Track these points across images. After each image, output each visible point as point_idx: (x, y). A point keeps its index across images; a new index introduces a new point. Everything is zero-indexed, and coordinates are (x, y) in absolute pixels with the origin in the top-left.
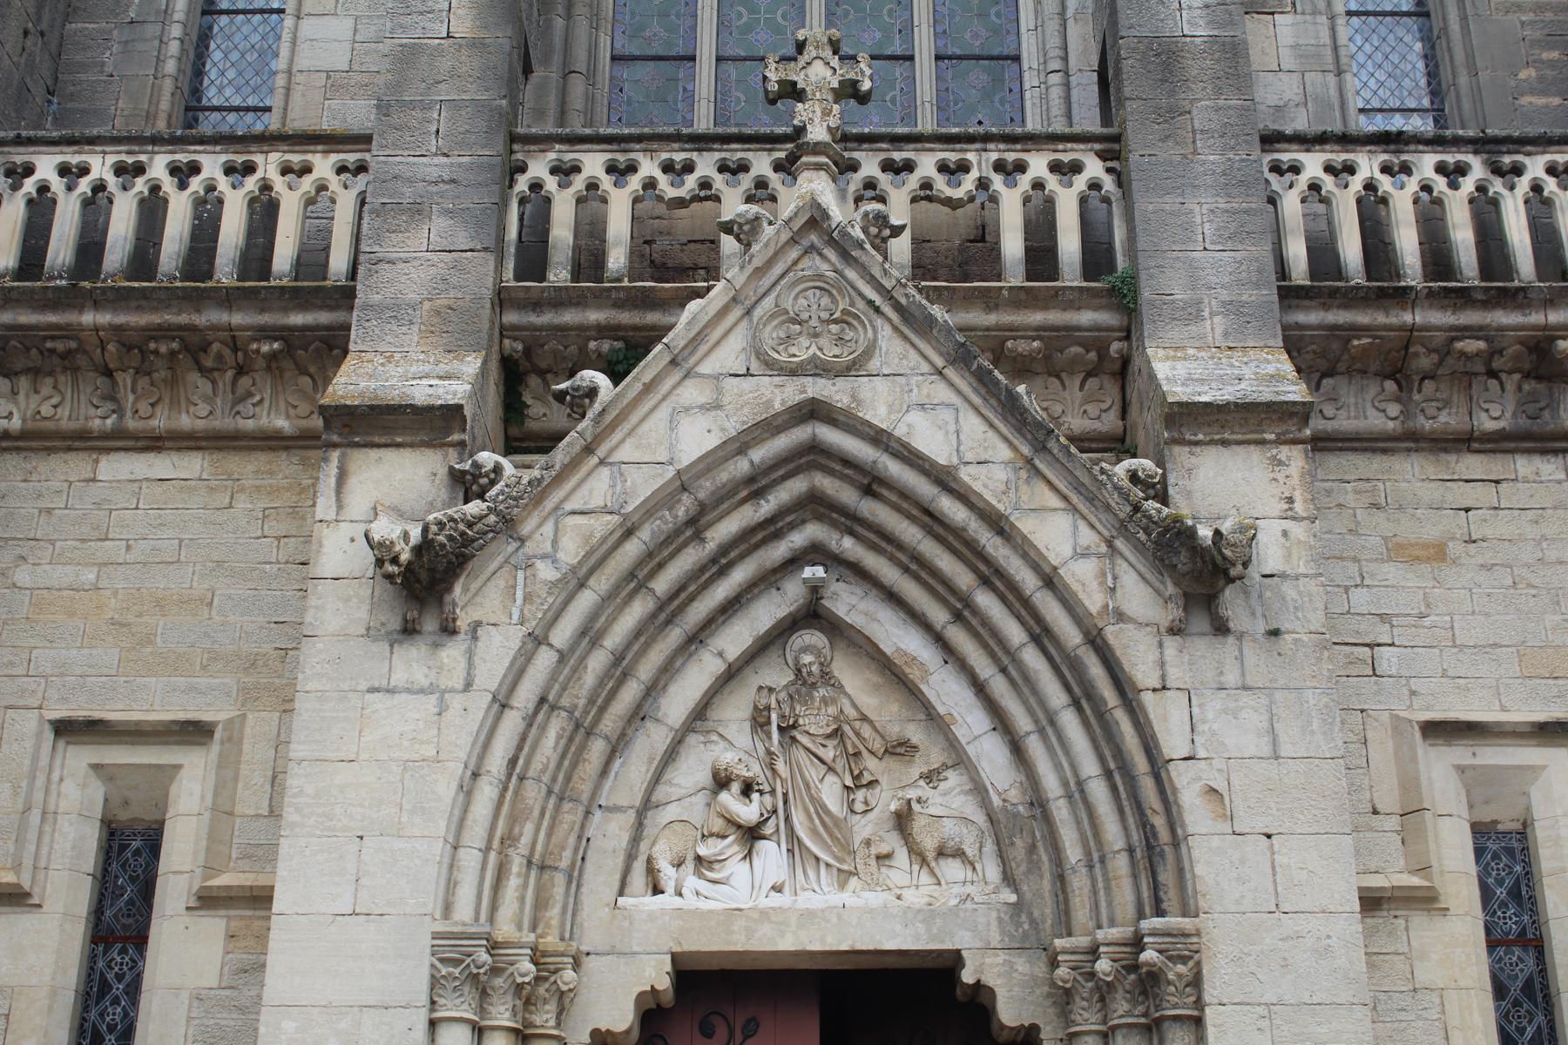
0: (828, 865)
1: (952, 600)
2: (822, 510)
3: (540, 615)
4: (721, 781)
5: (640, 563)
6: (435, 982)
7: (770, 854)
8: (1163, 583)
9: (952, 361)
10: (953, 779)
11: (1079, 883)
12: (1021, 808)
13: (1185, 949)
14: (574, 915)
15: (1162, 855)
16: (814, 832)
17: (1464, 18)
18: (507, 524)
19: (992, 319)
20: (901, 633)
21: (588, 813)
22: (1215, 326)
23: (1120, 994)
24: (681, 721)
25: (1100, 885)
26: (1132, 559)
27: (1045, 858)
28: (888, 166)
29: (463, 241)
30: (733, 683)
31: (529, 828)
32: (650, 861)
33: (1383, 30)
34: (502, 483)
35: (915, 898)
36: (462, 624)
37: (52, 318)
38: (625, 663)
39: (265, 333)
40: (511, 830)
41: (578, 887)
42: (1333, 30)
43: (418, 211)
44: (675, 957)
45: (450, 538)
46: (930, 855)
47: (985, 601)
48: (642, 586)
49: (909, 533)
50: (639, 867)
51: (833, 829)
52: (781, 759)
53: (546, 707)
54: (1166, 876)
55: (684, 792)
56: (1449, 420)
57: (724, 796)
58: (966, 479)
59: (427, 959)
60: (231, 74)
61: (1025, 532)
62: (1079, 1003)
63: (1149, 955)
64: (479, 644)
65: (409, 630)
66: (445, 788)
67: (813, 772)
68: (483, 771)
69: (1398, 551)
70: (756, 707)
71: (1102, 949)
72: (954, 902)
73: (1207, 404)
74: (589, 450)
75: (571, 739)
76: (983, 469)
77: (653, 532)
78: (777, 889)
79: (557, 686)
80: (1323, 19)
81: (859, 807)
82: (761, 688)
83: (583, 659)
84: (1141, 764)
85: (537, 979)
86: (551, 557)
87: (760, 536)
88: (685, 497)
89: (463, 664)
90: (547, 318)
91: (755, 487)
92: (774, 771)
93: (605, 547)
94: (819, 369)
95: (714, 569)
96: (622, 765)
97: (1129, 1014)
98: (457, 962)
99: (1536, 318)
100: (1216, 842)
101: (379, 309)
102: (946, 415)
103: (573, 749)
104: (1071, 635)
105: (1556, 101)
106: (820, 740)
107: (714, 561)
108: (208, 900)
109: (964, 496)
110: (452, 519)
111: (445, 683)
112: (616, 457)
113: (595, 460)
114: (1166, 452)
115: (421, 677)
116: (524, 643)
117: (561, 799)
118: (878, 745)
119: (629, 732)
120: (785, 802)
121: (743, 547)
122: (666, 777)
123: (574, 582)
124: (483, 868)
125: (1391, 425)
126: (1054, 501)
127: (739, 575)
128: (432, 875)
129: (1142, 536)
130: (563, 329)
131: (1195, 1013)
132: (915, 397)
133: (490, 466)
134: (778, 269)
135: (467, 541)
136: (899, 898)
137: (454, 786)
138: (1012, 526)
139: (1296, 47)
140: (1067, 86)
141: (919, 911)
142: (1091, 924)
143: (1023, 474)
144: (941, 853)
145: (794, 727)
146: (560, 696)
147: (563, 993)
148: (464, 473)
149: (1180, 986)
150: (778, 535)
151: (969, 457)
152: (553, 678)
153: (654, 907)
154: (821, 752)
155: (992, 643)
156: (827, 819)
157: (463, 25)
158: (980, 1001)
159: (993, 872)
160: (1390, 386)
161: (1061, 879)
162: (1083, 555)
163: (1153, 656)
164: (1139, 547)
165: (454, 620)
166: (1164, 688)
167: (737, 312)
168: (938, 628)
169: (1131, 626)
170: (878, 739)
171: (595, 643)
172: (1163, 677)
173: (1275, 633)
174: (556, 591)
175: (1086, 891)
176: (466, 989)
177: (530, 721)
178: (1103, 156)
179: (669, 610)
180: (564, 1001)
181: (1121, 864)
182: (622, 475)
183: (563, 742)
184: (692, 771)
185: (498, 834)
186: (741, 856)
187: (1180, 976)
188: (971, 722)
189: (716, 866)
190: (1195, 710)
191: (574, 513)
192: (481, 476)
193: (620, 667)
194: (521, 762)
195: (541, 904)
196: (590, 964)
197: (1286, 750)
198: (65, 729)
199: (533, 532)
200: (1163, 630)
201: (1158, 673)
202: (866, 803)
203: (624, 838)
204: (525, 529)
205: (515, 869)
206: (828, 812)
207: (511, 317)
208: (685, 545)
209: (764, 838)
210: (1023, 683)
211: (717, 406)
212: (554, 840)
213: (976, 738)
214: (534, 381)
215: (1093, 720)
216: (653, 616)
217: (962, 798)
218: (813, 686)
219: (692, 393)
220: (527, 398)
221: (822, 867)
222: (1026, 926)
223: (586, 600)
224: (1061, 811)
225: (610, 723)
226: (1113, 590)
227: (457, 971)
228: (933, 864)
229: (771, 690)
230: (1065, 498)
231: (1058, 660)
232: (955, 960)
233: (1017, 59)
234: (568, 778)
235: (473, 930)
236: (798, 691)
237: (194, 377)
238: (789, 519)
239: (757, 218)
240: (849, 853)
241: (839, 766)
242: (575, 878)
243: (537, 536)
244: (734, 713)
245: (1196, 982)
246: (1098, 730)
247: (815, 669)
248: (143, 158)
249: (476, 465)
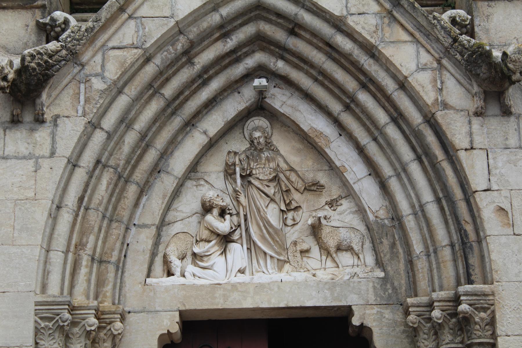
0: (271, 257)
1: (344, 97)
2: (265, 44)
3: (95, 111)
5: (155, 78)
6: (37, 331)
8: (472, 85)
10: (346, 205)
11: (421, 265)
12: (386, 222)
14: (120, 289)
15: (471, 248)
16: (263, 238)
20: (313, 118)
21: (127, 229)
23: (446, 331)
24: (182, 173)
25: (434, 266)
26: (452, 71)
27: (401, 251)
30: (213, 149)
31: (92, 239)
32: (165, 256)
34: (69, 31)
36: (48, 116)
38: (147, 139)
40: (81, 239)
41: (123, 273)
44: (181, 313)
45: (39, 64)
46: (332, 250)
47: (364, 97)
48: (157, 92)
50: (159, 260)
52: (243, 194)
53: (100, 166)
54: (474, 260)
55: (185, 215)
57: (209, 218)
58: (352, 24)
59: (32, 318)
61: (388, 56)
63: (464, 307)
64: (59, 129)
67: (262, 202)
68: (63, 205)
70: (227, 164)
71: (436, 304)
72: (347, 277)
75: (116, 185)
76: (361, 18)
77: (162, 59)
78: (242, 271)
79: (106, 154)
81: (290, 222)
82: (229, 152)
83: (122, 136)
84: (458, 194)
85: (99, 328)
86: (101, 76)
87: (227, 61)
88: (181, 37)
89: (49, 141)
91: (224, 31)
92: (238, 202)
93: (133, 69)
95: (200, 81)
96: (147, 200)
97: (452, 342)
98: (50, 319)
100: (503, 239)
103: (117, 191)
106: (265, 183)
107: (199, 76)
109: (351, 35)
110: (39, 53)
111: (38, 153)
112: (139, 14)
113: (125, 16)
114: (474, 5)
115: (23, 149)
116: (86, 128)
117: (111, 221)
118: (300, 185)
119: (151, 180)
120: (246, 220)
121: (217, 68)
122: (174, 206)
123: (115, 90)
124: (65, 263)
126: (404, 36)
127: (215, 85)
129: (458, 57)
131: (492, 341)
133: (61, 20)
135: (49, 66)
136: (314, 275)
137: (46, 214)
138: (380, 52)
141: (326, 283)
142: (429, 289)
143: (386, 20)
144: (339, 249)
145: (250, 175)
146: (108, 159)
147: (114, 336)
148: (45, 24)
149: (483, 325)
150: (238, 60)
151: (353, 10)
152: (104, 148)
153: (168, 284)
154: (266, 190)
155: (368, 123)
156: (270, 230)
159: (369, 259)
161: (410, 263)
162: (423, 69)
163: (465, 129)
164: (456, 63)
165: (43, 115)
166: (472, 148)
168: (336, 114)
169: (452, 112)
170: (300, 181)
171: (129, 127)
172: (471, 142)
174: (104, 96)
175: (426, 270)
176: (57, 335)
181: (446, 253)
182: (142, 24)
183: (111, 187)
185: (73, 242)
186: (219, 252)
187: (482, 319)
189: (205, 259)
190: (491, 161)
191: (114, 48)
192: (56, 26)
194: (86, 199)
195: (100, 283)
196: (131, 318)
199: (89, 60)
200: (471, 113)
201: (468, 139)
202: (294, 220)
203: (150, 243)
204: (85, 58)
205: (84, 263)
206: (271, 226)
208: (182, 67)
209: (233, 241)
212: (107, 245)
213: (359, 180)
215: (429, 168)
216: (164, 110)
217: (351, 216)
218: (261, 150)
221: (268, 258)
222: (390, 291)
223: (123, 101)
224: (410, 223)
225: (139, 175)
226: (441, 90)
227: (50, 325)
228: (334, 255)
229: (236, 153)
230: (412, 35)
231: (408, 132)
232: (348, 311)
234: (115, 208)
235: (60, 299)
236: (252, 154)
238: (244, 50)
240: (284, 250)
241: (277, 198)
243: (92, 63)
245: (492, 322)
246: (432, 174)
247: (262, 140)
249: (53, 20)
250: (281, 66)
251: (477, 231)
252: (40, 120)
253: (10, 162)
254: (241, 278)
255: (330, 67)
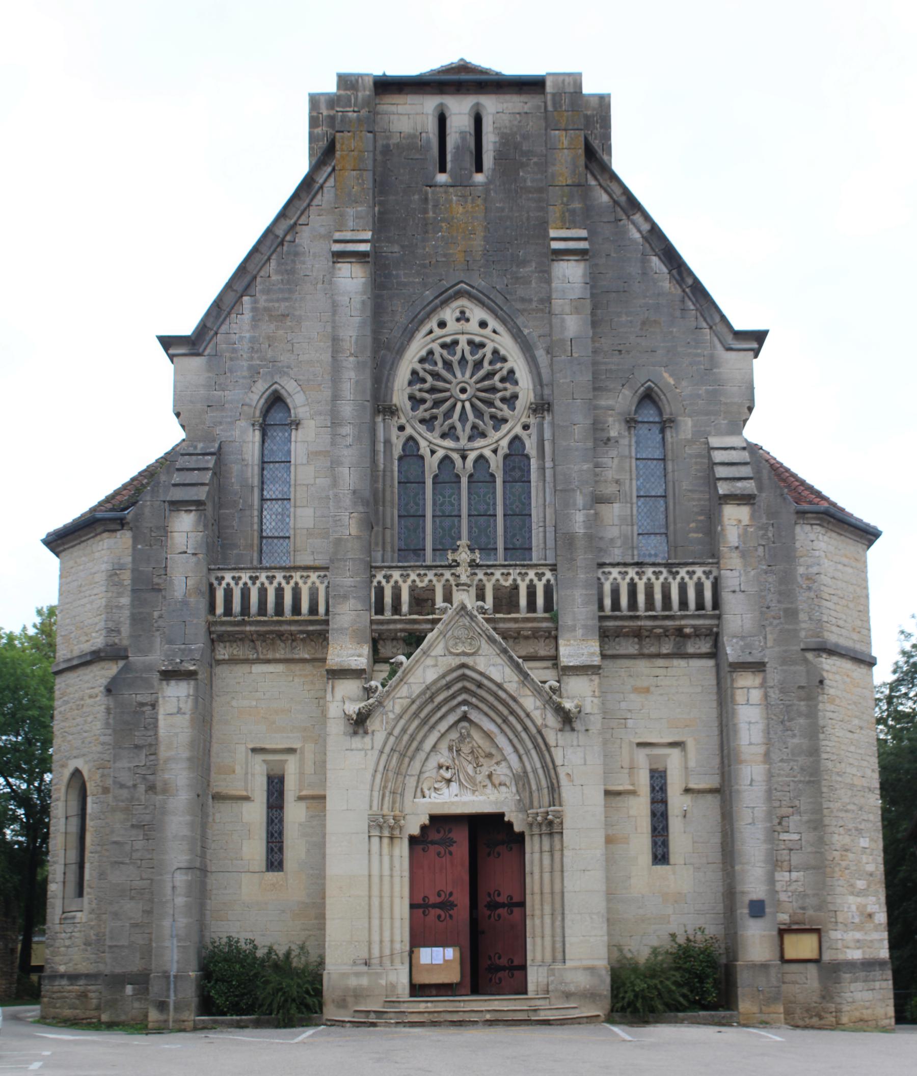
4: (440, 767)
6: (369, 826)
7: (454, 785)
9: (501, 652)
10: (504, 764)
11: (535, 795)
13: (559, 815)
17: (674, 504)
18: (380, 703)
19: (516, 626)
22: (580, 632)
28: (486, 574)
29: (360, 607)
33: (651, 503)
35: (492, 798)
36: (370, 731)
37: (237, 629)
39: (301, 632)
42: (632, 508)
43: (345, 597)
47: (512, 719)
49: (491, 699)
50: (419, 790)
51: (472, 780)
54: (556, 796)
56: (653, 650)
57: (441, 771)
60: (273, 524)
62: (534, 826)
63: (550, 817)
65: (355, 733)
66: (368, 776)
67: (465, 763)
69: (636, 690)
73: (572, 666)
74: (401, 680)
80: (629, 505)
86: (392, 711)
89: (370, 742)
90: (385, 627)
94: (464, 654)
99: (677, 623)
101: (337, 630)
102: (500, 668)
104: (533, 730)
105: (700, 535)
108: (301, 798)
109: (505, 691)
115: (360, 746)
118: (483, 754)
125: (636, 652)
126: (530, 693)
127: (444, 710)
128: (367, 799)
130: (390, 630)
132: (491, 662)
134: (452, 623)
139: (619, 516)
140: (545, 532)
144: (500, 784)
157: (354, 531)
158: (510, 825)
159: (514, 789)
160: (636, 640)
161: (531, 793)
163: (554, 737)
167: (441, 637)
173: (587, 730)
177: (389, 756)
178: (551, 570)
179: (424, 722)
180: (401, 828)
181: (545, 791)
184: (432, 763)
188: (508, 750)
193: (412, 738)
195: (394, 802)
196: (408, 817)
197: (588, 762)
198: (254, 750)
203: (415, 784)
204: (385, 704)
207: (374, 627)
210: (521, 741)
211: (436, 665)
214: (381, 642)
219: (429, 661)
220: (379, 647)
223: (402, 722)
224: (531, 776)
225: (410, 753)
232: (502, 815)
233: (530, 515)
237: (279, 642)
239: (446, 607)
242: (402, 795)
244: (443, 746)
245: (562, 823)
248: (258, 574)
250: (474, 700)
251: (558, 782)
252: (366, 733)
253: (354, 752)
254: (456, 799)
255: (496, 703)
